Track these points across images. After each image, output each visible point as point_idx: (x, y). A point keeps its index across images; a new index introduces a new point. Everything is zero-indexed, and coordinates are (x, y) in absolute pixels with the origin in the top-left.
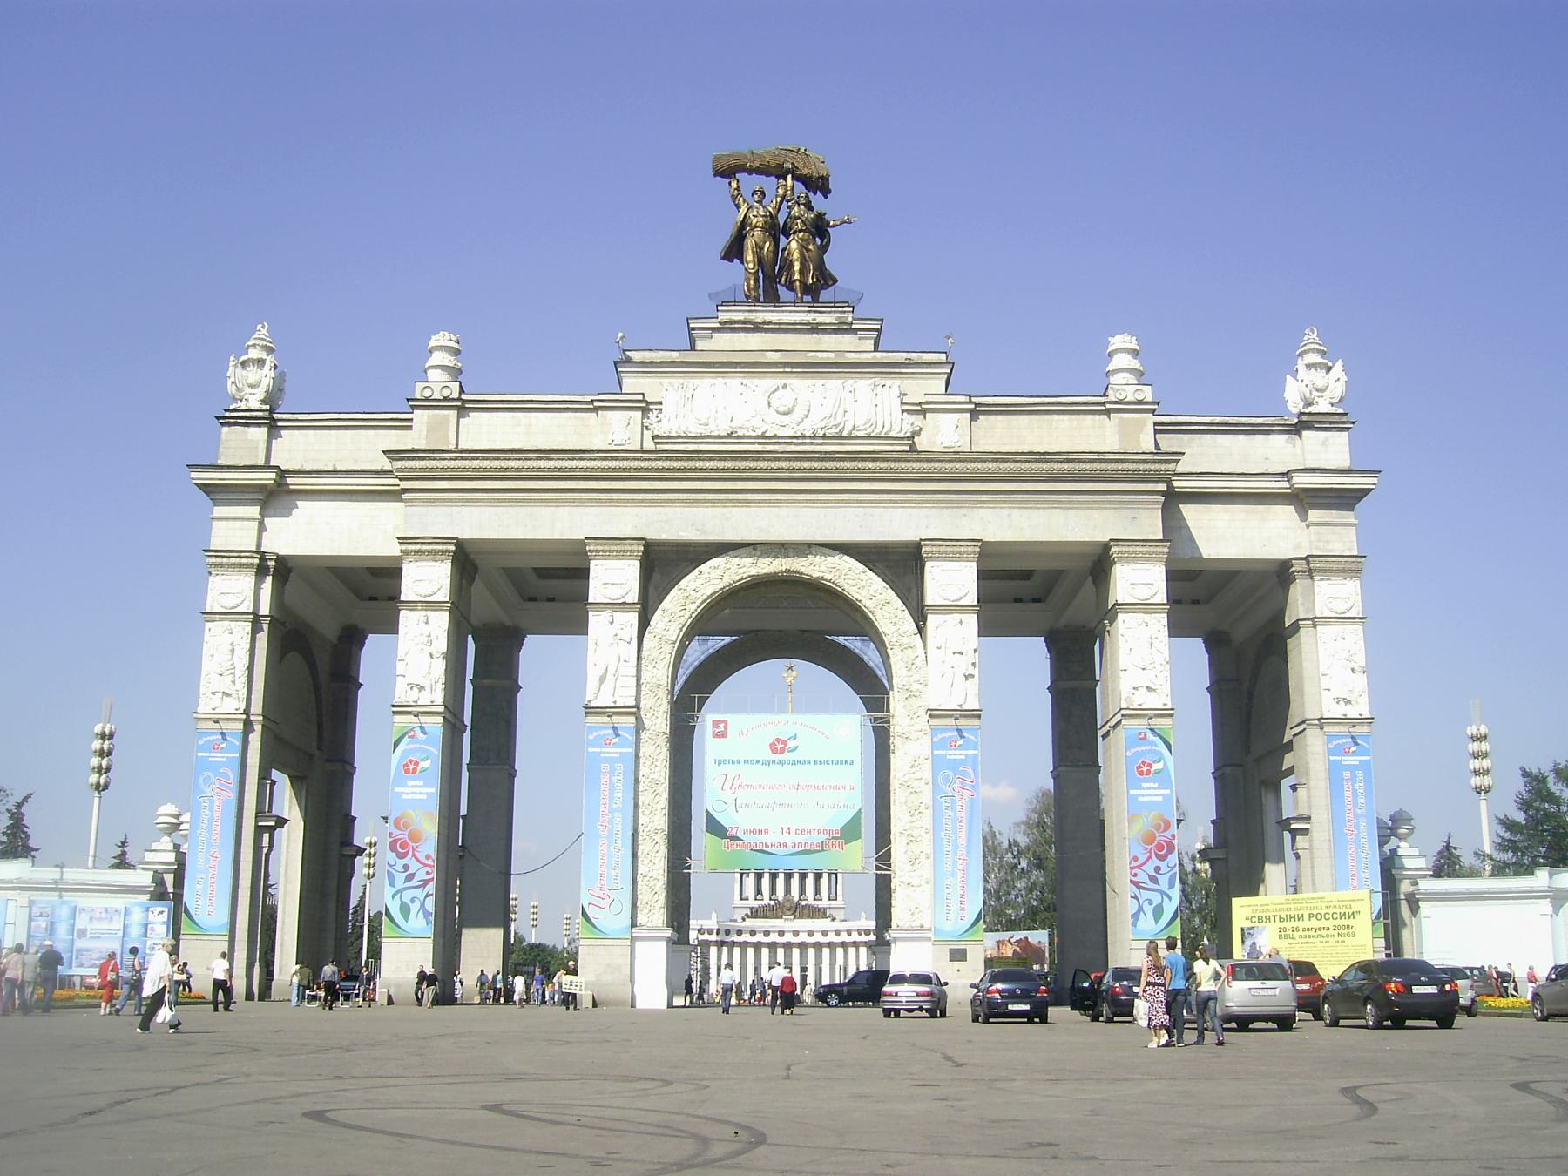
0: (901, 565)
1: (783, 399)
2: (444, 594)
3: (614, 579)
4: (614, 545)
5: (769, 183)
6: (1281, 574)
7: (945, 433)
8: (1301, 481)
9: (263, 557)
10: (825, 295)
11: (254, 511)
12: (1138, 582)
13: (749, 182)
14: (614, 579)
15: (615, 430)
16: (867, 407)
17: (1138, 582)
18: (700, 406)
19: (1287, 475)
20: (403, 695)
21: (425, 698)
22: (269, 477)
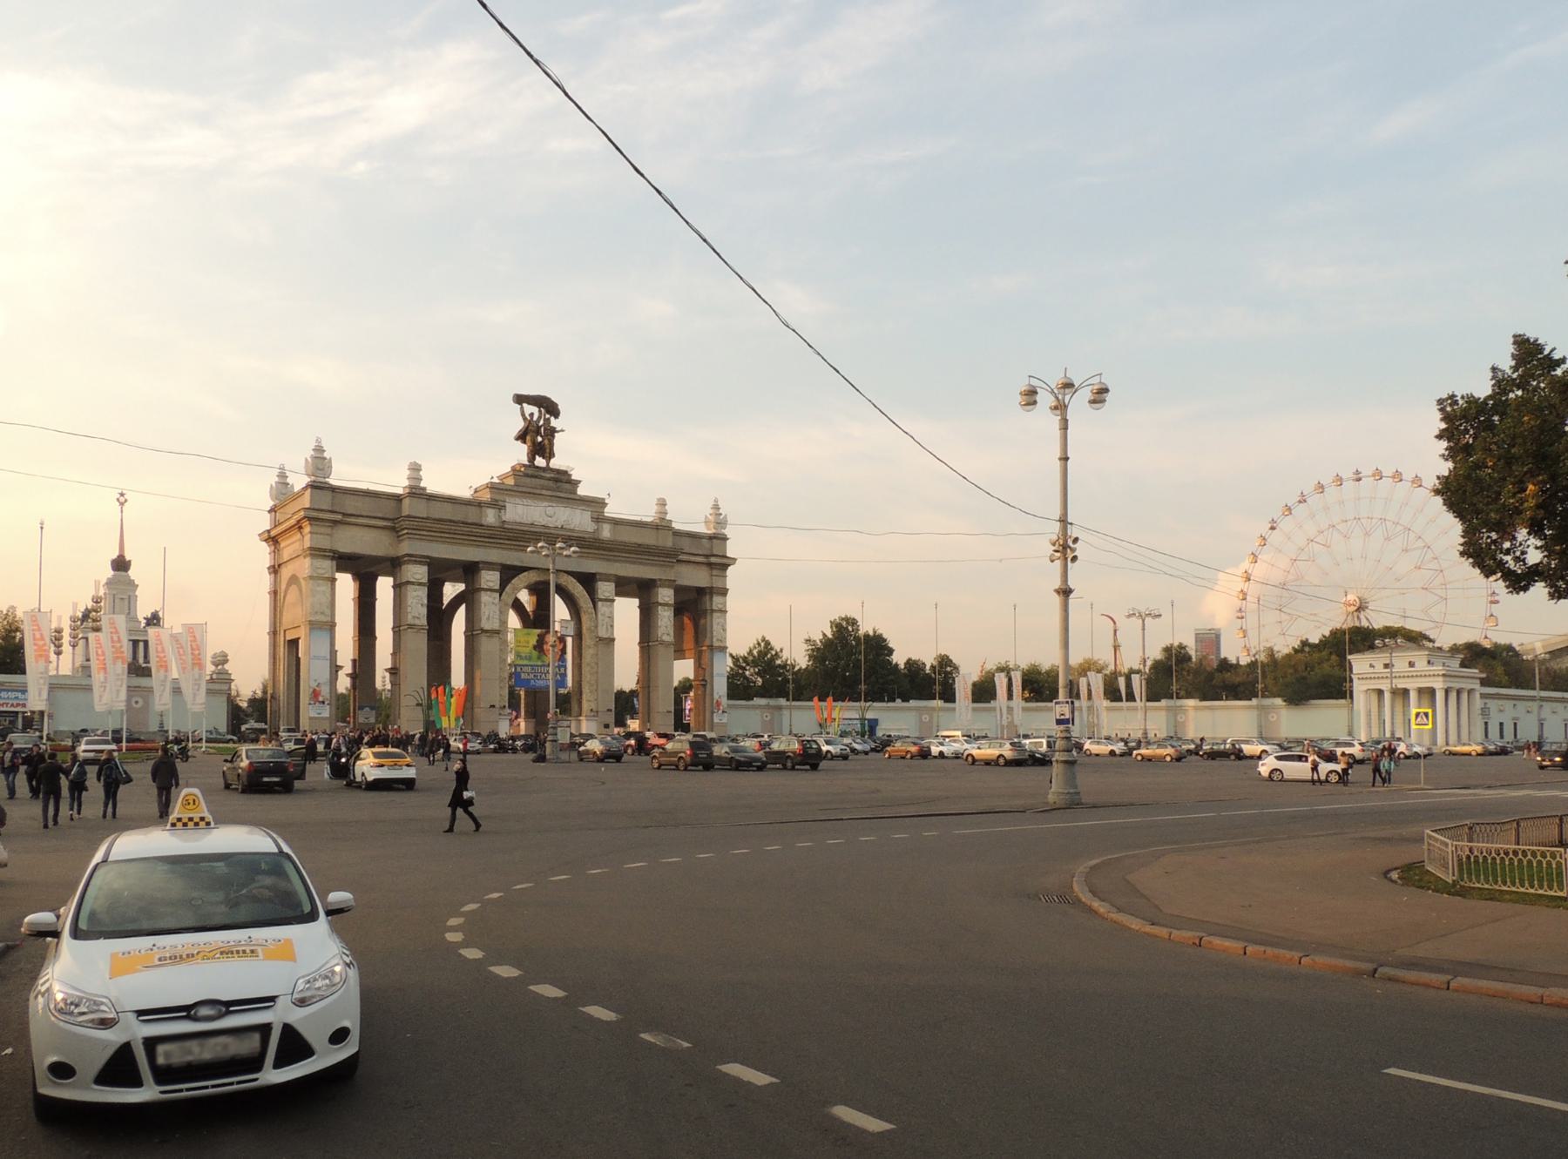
0: (588, 581)
1: (550, 510)
2: (425, 580)
3: (490, 578)
4: (490, 566)
5: (535, 410)
6: (701, 591)
7: (606, 532)
8: (713, 560)
9: (334, 552)
10: (554, 463)
11: (328, 530)
12: (666, 595)
13: (530, 409)
14: (490, 578)
15: (490, 517)
16: (579, 520)
17: (666, 595)
18: (521, 512)
19: (707, 556)
20: (410, 620)
21: (417, 622)
22: (339, 517)
